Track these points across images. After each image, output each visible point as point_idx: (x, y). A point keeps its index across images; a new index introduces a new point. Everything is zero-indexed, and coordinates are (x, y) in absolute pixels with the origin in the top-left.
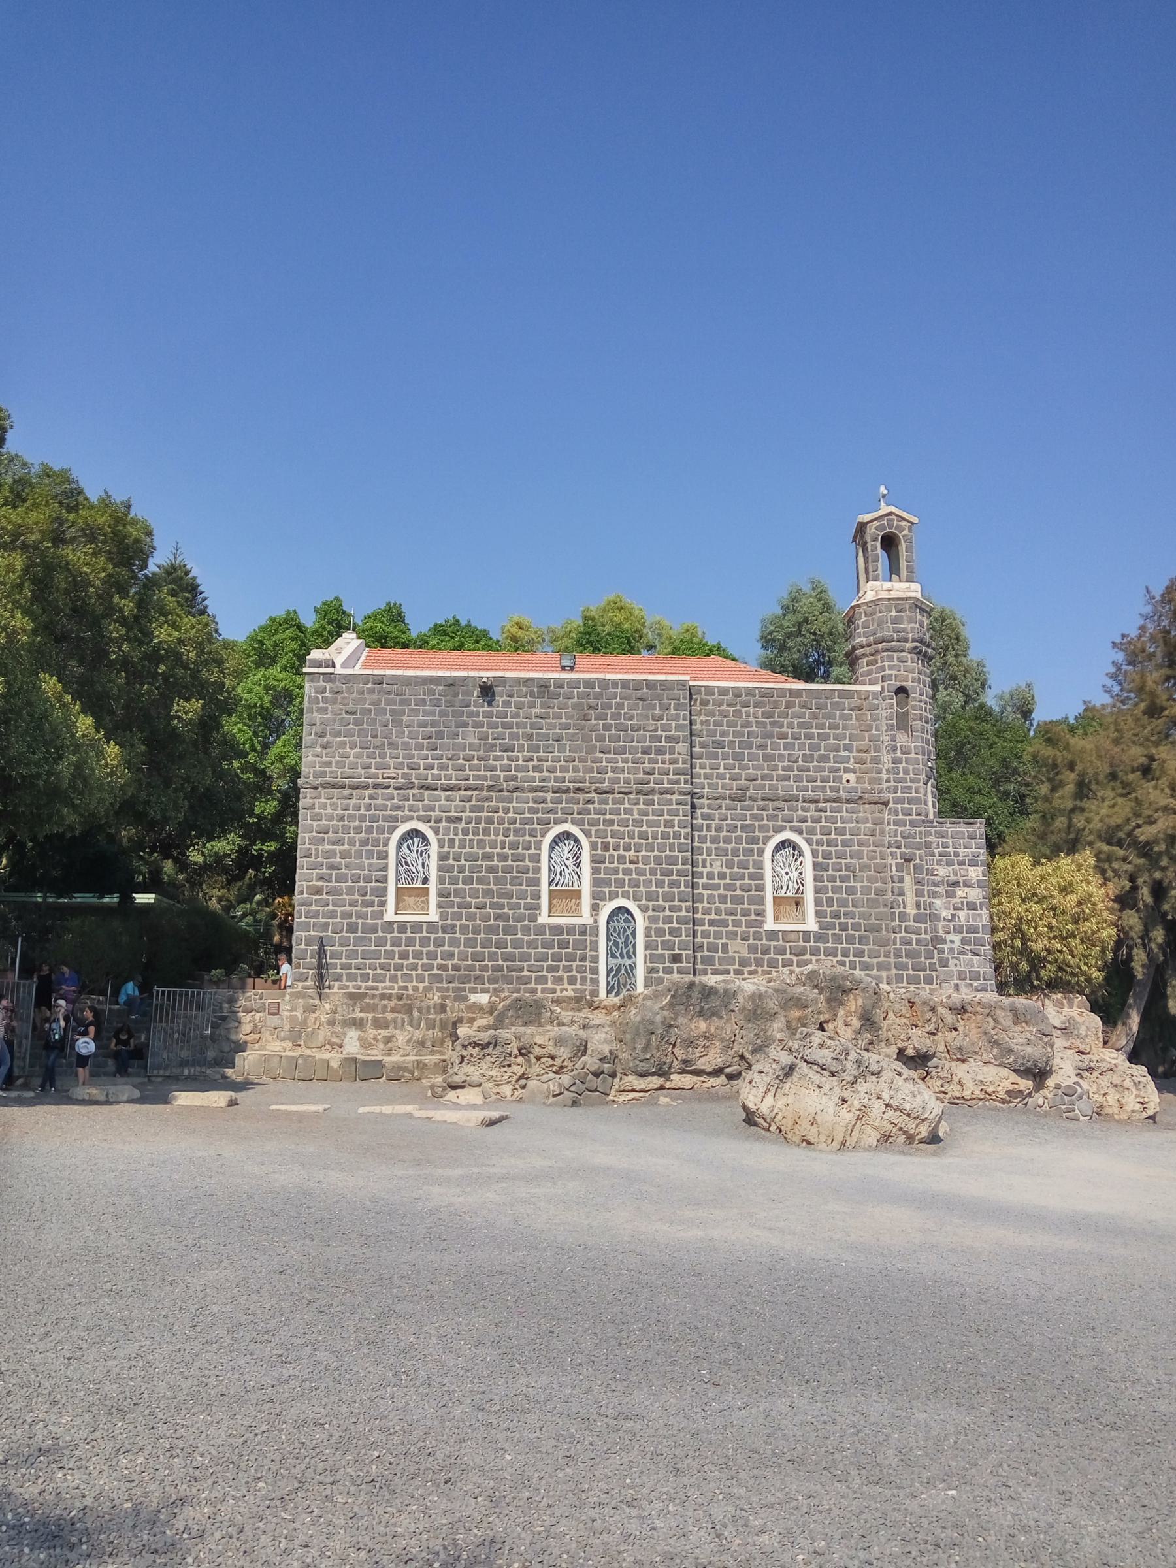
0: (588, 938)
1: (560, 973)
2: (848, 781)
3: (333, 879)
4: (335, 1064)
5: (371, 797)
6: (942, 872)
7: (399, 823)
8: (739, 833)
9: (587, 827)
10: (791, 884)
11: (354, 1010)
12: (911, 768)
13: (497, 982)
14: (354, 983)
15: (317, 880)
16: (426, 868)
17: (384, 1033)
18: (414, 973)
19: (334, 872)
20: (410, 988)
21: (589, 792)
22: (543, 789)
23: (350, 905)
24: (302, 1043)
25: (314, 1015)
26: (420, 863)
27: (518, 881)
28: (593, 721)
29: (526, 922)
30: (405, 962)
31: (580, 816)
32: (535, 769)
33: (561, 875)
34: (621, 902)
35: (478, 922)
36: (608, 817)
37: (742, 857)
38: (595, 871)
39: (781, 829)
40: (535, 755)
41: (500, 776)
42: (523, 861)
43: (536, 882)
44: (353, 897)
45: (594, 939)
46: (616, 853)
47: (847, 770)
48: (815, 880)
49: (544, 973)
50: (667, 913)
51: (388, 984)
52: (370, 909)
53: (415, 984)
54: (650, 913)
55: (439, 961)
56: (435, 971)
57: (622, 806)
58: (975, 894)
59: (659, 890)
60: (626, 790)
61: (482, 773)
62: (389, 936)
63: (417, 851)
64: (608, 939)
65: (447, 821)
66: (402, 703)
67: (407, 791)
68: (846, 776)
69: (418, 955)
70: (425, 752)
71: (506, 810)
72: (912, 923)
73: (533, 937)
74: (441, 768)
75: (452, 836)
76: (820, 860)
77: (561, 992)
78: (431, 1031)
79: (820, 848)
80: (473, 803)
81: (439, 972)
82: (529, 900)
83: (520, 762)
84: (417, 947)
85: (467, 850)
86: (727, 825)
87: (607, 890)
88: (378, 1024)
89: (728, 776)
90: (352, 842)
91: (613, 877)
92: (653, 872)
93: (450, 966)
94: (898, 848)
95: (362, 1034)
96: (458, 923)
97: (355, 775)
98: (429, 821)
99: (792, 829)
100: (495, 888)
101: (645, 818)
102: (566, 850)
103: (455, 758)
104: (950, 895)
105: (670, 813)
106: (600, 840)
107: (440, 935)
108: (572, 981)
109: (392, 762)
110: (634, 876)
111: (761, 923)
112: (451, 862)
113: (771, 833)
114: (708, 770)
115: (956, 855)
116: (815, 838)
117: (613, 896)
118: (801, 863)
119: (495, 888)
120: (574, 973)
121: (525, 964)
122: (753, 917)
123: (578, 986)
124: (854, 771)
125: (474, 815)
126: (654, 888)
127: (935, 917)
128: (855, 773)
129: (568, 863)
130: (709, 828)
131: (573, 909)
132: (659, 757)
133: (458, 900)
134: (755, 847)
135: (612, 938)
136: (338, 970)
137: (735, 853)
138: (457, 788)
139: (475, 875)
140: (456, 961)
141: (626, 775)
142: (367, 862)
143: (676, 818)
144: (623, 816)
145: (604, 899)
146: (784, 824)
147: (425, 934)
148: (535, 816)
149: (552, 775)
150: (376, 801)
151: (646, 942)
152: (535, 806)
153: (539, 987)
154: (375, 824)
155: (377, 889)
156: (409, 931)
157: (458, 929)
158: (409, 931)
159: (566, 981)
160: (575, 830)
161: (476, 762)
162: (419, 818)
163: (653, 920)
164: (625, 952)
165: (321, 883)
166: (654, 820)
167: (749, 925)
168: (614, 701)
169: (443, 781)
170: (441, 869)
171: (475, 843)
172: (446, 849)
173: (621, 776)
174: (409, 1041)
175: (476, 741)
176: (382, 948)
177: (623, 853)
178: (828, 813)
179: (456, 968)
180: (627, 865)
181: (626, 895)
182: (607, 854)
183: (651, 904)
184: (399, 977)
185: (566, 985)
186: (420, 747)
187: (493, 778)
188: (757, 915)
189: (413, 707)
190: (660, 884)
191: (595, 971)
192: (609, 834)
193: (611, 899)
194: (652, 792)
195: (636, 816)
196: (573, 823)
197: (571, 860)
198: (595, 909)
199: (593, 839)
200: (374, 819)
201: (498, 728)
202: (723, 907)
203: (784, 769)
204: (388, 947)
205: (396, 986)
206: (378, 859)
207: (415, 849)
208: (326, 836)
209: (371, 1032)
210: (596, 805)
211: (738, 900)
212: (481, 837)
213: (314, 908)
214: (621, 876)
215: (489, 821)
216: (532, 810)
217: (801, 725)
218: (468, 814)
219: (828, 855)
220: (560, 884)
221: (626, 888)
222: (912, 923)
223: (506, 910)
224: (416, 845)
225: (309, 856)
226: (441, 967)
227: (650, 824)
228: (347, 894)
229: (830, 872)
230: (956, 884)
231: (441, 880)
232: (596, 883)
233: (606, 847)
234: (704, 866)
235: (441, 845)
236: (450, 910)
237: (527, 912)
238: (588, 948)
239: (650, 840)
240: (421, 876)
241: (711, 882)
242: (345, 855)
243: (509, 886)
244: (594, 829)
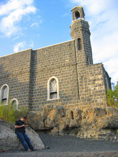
2: (67, 62)
6: (91, 78)
10: (55, 89)
38: (10, 93)
39: (51, 76)
47: (67, 59)
54: (20, 101)
58: (100, 82)
68: (66, 61)
92: (21, 91)
99: (54, 76)
104: (94, 83)
115: (95, 73)
117: (13, 98)
122: (45, 98)
124: (68, 59)
127: (90, 90)
163: (20, 102)
167: (44, 100)
181: (15, 97)
188: (45, 98)
190: (22, 93)
202: (38, 97)
203: (52, 62)
211: (41, 95)
230: (95, 80)
233: (12, 87)
234: (34, 88)
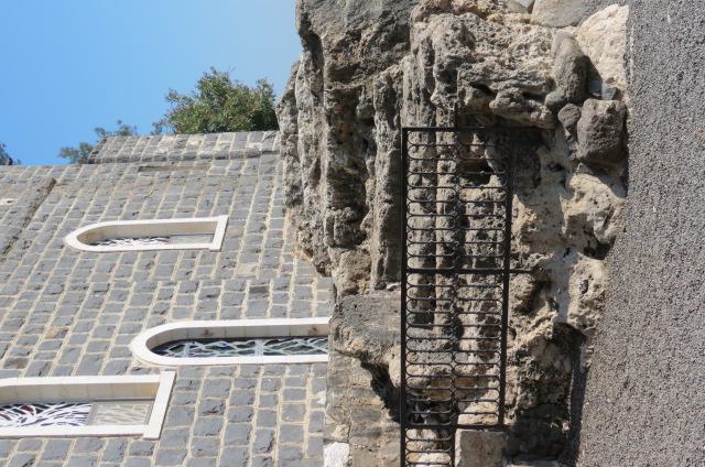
1: (279, 410)
38: (63, 371)
49: (277, 430)
72: (227, 168)
77: (320, 406)
87: (107, 361)
111: (208, 254)
123: (309, 387)
126: (122, 314)
153: (307, 435)
177: (39, 343)
180: (66, 341)
193: (131, 355)
222: (227, 168)
232: (91, 367)
238: (228, 377)
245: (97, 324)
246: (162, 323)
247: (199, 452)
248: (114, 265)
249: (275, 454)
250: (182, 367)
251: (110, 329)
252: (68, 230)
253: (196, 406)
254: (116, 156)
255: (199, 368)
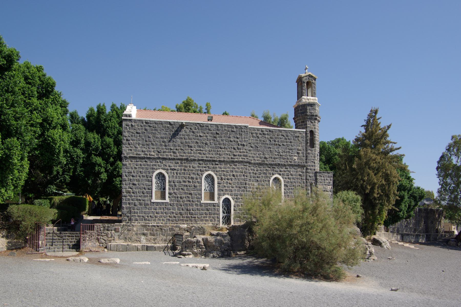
0: (216, 207)
1: (208, 218)
3: (134, 188)
4: (139, 247)
5: (146, 161)
7: (155, 170)
8: (262, 175)
9: (216, 172)
11: (144, 230)
12: (313, 156)
13: (188, 221)
14: (142, 222)
15: (128, 188)
16: (164, 185)
17: (153, 237)
18: (161, 218)
19: (134, 186)
20: (160, 223)
21: (217, 161)
22: (202, 160)
23: (140, 197)
24: (127, 240)
25: (131, 232)
26: (162, 183)
27: (195, 189)
28: (218, 139)
29: (197, 203)
30: (158, 215)
31: (214, 169)
32: (200, 153)
33: (208, 187)
34: (227, 196)
35: (182, 202)
36: (223, 169)
37: (263, 182)
38: (219, 186)
40: (200, 149)
41: (188, 155)
42: (196, 183)
43: (201, 190)
44: (141, 194)
45: (218, 208)
46: (225, 181)
47: (295, 156)
48: (284, 190)
50: (241, 200)
51: (153, 222)
52: (146, 198)
53: (162, 222)
55: (169, 215)
56: (168, 218)
57: (227, 166)
59: (238, 193)
60: (229, 161)
61: (182, 154)
62: (153, 207)
63: (161, 179)
64: (223, 208)
65: (171, 170)
66: (156, 130)
67: (157, 160)
69: (162, 213)
70: (163, 147)
71: (190, 167)
73: (199, 207)
74: (168, 152)
75: (173, 175)
76: (286, 184)
78: (169, 237)
79: (286, 180)
80: (180, 164)
81: (169, 218)
82: (197, 196)
83: (195, 151)
84: (162, 210)
85: (178, 179)
86: (259, 172)
87: (222, 192)
88: (151, 234)
89: (259, 157)
90: (139, 177)
91: (224, 189)
92: (236, 187)
93: (173, 216)
94: (308, 180)
95: (147, 238)
96: (175, 203)
97: (141, 154)
98: (165, 170)
100: (187, 191)
101: (234, 170)
102: (209, 179)
103: (173, 149)
105: (242, 168)
106: (220, 177)
107: (170, 206)
108: (211, 221)
109: (152, 150)
110: (231, 188)
112: (172, 183)
113: (272, 175)
114: (253, 155)
116: (285, 176)
118: (280, 184)
119: (187, 191)
120: (212, 218)
121: (196, 216)
123: (213, 222)
125: (179, 168)
126: (237, 192)
128: (297, 157)
129: (210, 184)
130: (253, 173)
131: (211, 198)
132: (239, 151)
133: (175, 195)
134: (267, 179)
135: (223, 207)
136: (137, 218)
137: (261, 181)
138: (174, 159)
139: (180, 187)
140: (175, 215)
141: (229, 156)
142: (145, 183)
143: (244, 170)
144: (227, 169)
145: (221, 195)
146: (275, 172)
147: (165, 206)
148: (199, 169)
149: (205, 155)
150: (148, 163)
151: (234, 209)
152: (200, 165)
153: (201, 222)
154: (147, 170)
155: (149, 192)
156: (159, 205)
157: (175, 205)
158: (159, 205)
159: (209, 221)
160: (212, 173)
161: (180, 151)
162: (162, 169)
163: (236, 202)
164: (227, 211)
165: (130, 189)
166: (237, 171)
168: (225, 132)
169: (170, 157)
170: (169, 185)
171: (180, 177)
172: (171, 179)
173: (227, 156)
174: (162, 240)
175: (180, 144)
176: (151, 211)
177: (228, 181)
178: (289, 169)
179: (174, 217)
180: (229, 185)
181: (228, 194)
182: (222, 181)
183: (236, 197)
184: (157, 219)
185: (209, 222)
186: (161, 145)
187: (186, 156)
189: (159, 131)
191: (218, 218)
192: (223, 175)
194: (237, 162)
195: (231, 170)
196: (212, 171)
197: (211, 183)
198: (219, 198)
199: (218, 176)
200: (147, 169)
201: (187, 139)
204: (153, 210)
205: (156, 222)
206: (148, 182)
207: (161, 179)
208: (131, 174)
209: (150, 237)
210: (219, 166)
212: (182, 175)
213: (128, 197)
214: (226, 188)
215: (184, 170)
216: (199, 167)
217: (281, 142)
218: (178, 168)
219: (288, 182)
220: (207, 190)
221: (228, 192)
223: (190, 199)
224: (161, 177)
225: (126, 181)
226: (169, 217)
227: (236, 172)
228: (139, 193)
229: (289, 187)
231: (169, 189)
232: (219, 190)
235: (169, 178)
236: (172, 199)
237: (197, 200)
239: (236, 177)
240: (163, 187)
241: (254, 190)
242: (139, 181)
243: (191, 191)
244: (218, 173)
245: (233, 189)
246: (233, 199)
247: (197, 209)
248: (264, 186)
249: (197, 218)
250: (219, 204)
251: (232, 191)
252: (280, 175)
253: (209, 207)
254: (318, 177)
255: (219, 206)
